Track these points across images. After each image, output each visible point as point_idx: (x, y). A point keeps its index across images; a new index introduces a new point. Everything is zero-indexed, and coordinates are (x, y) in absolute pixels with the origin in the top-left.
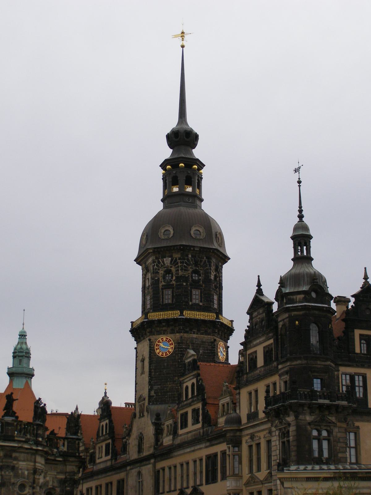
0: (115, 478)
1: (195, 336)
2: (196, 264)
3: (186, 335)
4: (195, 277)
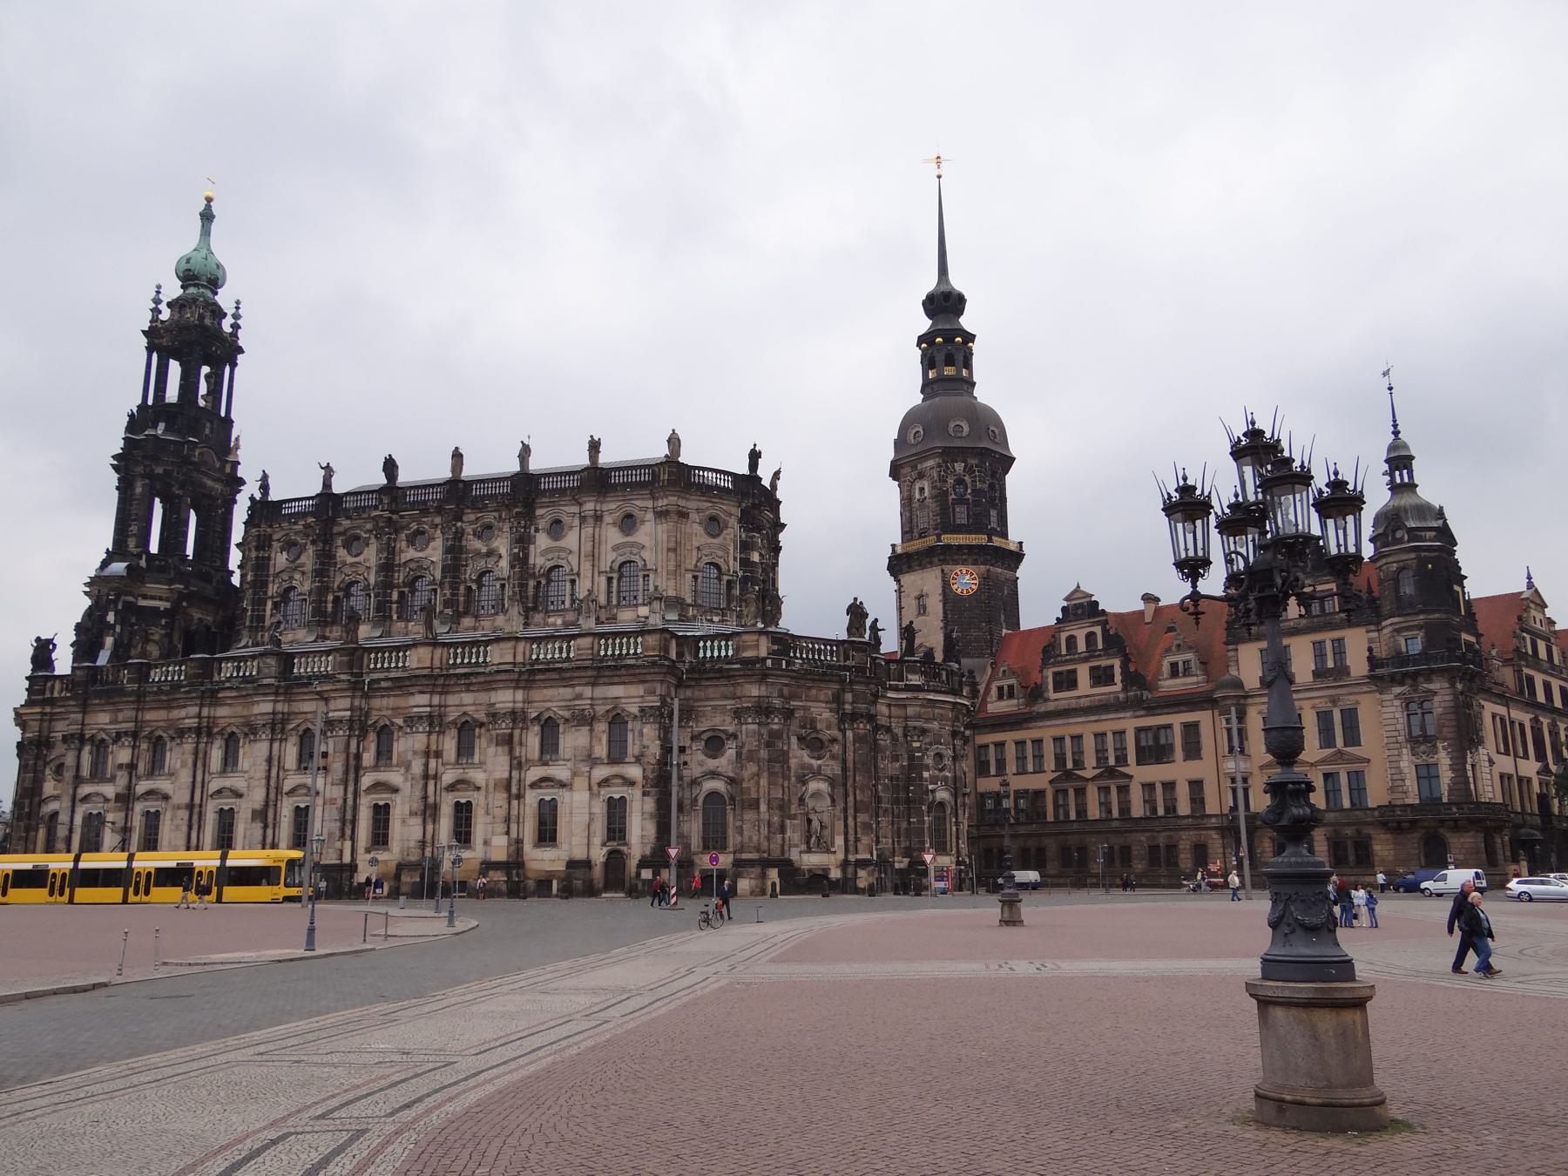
2: (993, 475)
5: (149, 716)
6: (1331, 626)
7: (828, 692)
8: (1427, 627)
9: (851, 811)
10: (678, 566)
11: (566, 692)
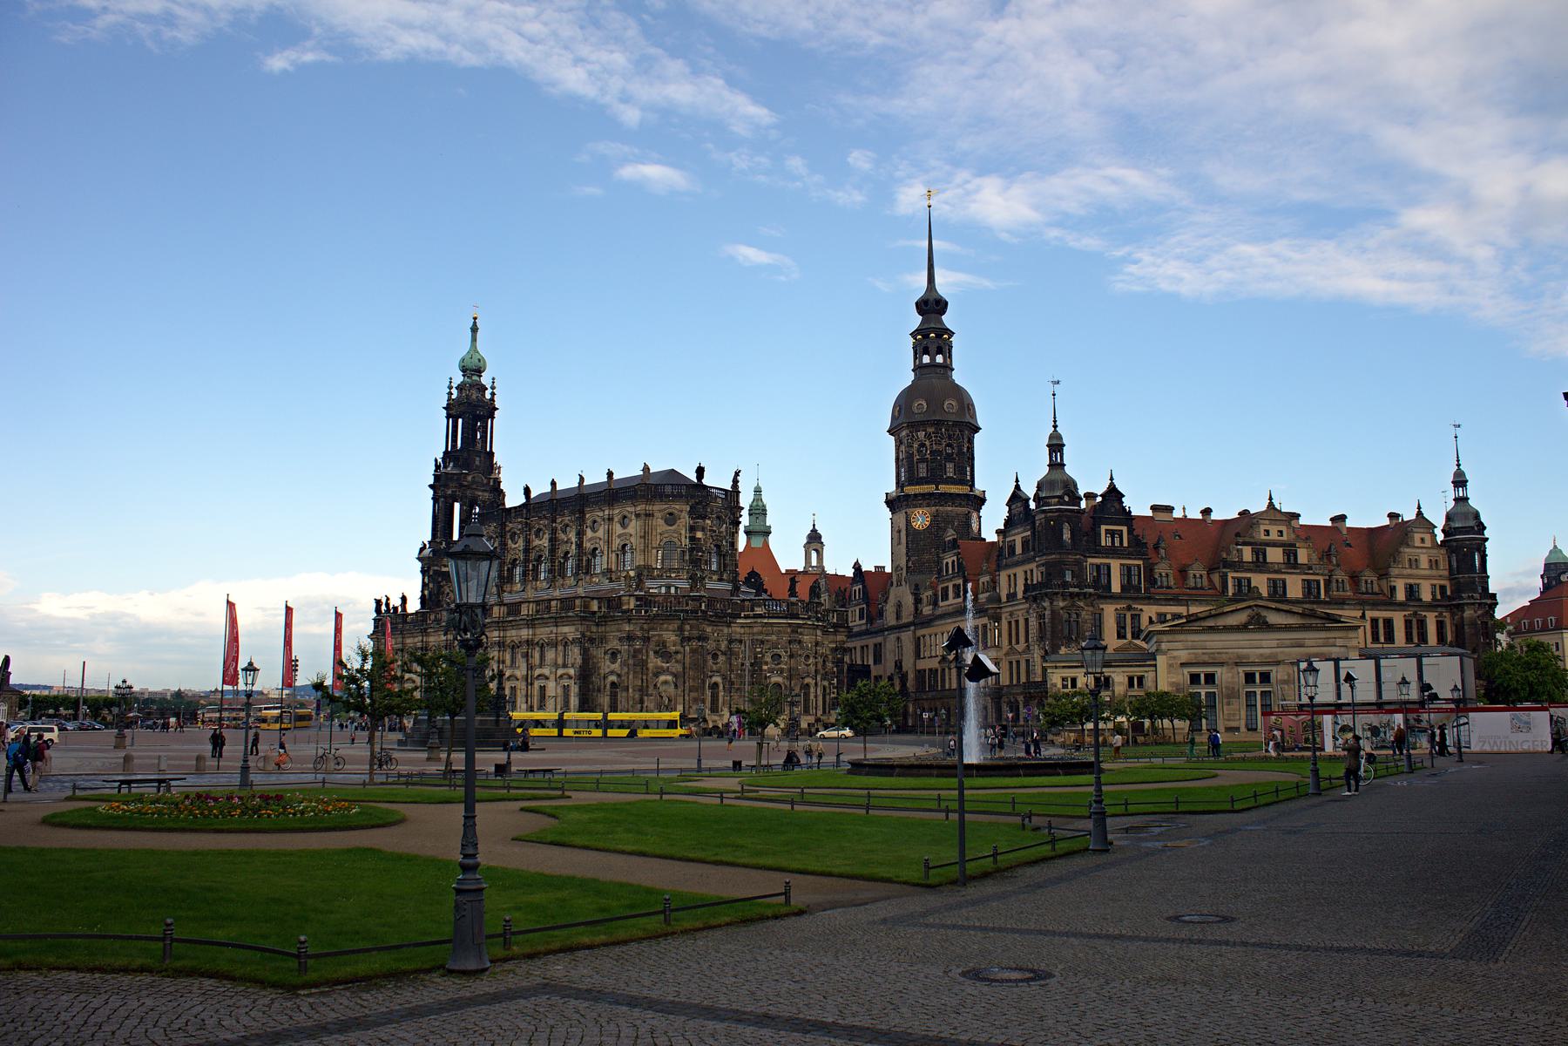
0: (871, 641)
2: (950, 437)
4: (949, 450)
5: (408, 641)
7: (675, 625)
10: (646, 546)
11: (548, 630)
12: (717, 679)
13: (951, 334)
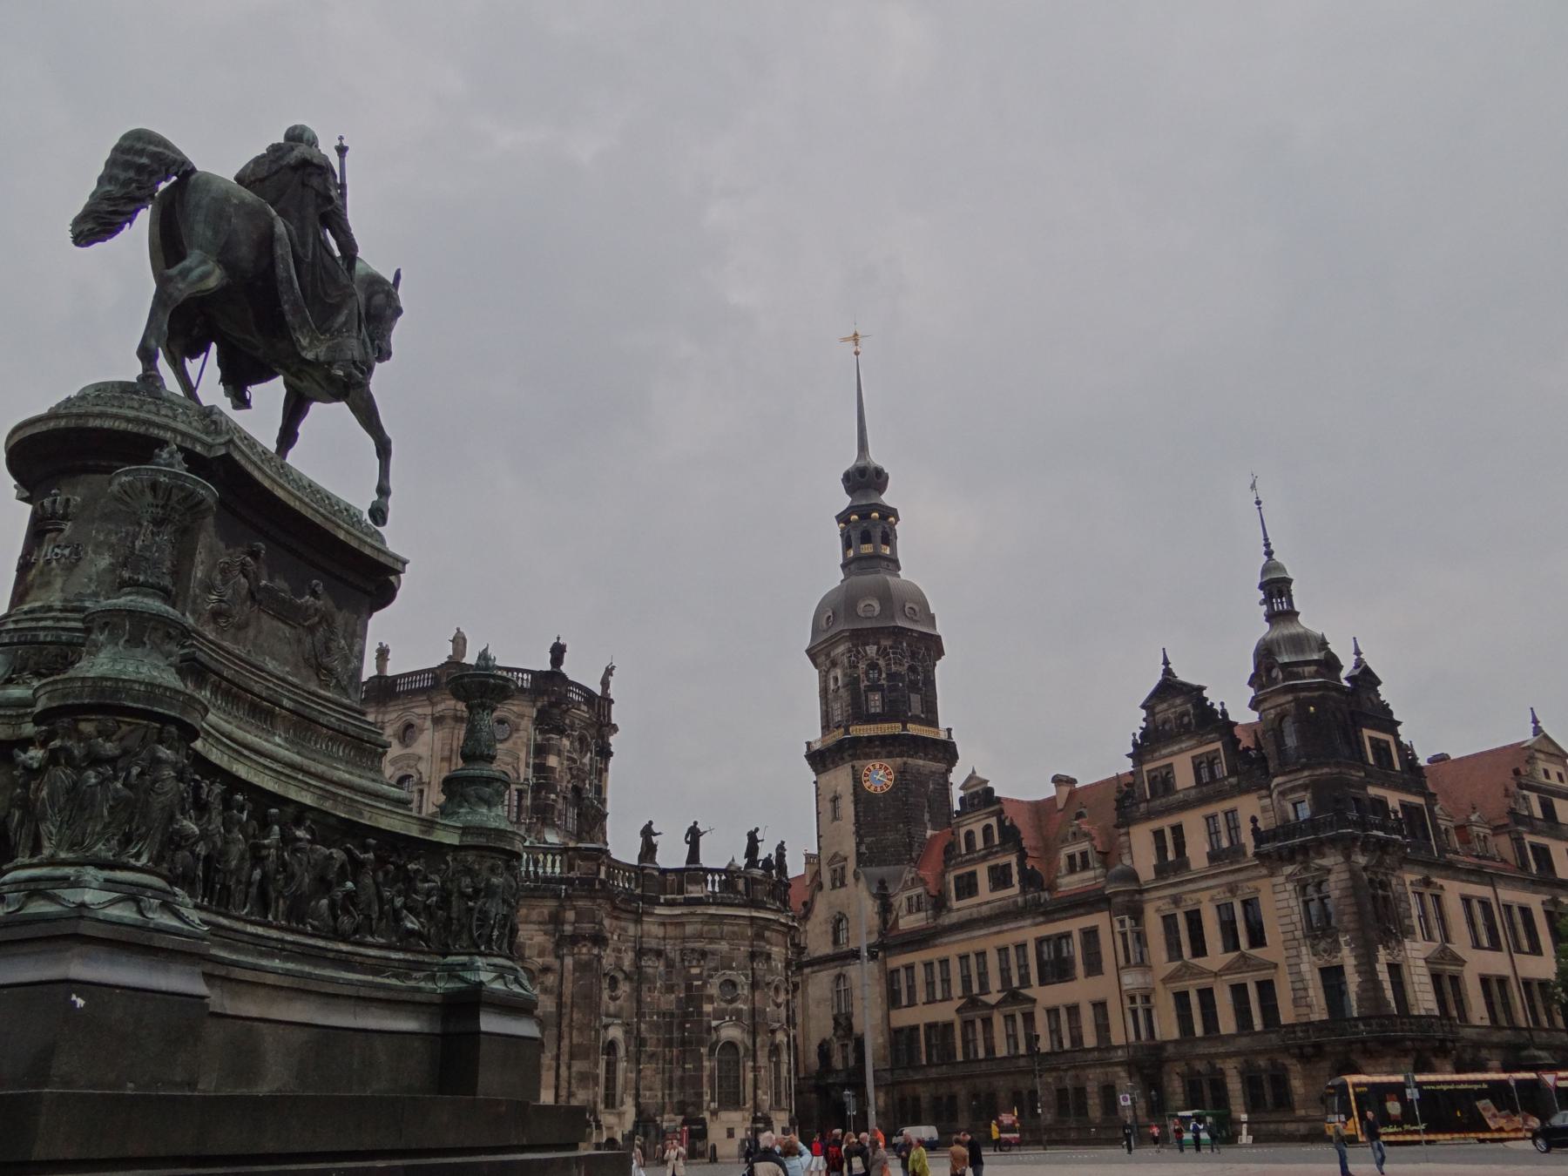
1: (921, 762)
2: (913, 655)
3: (910, 761)
6: (1221, 796)
8: (1316, 787)
9: (564, 1058)
12: (616, 1033)
13: (897, 519)
